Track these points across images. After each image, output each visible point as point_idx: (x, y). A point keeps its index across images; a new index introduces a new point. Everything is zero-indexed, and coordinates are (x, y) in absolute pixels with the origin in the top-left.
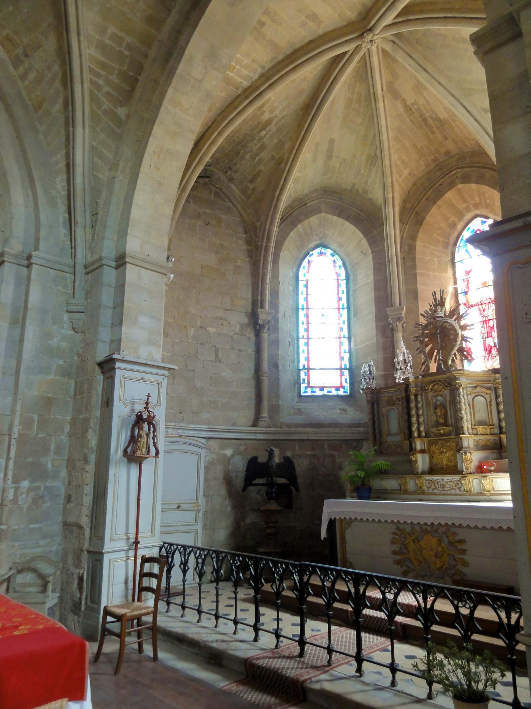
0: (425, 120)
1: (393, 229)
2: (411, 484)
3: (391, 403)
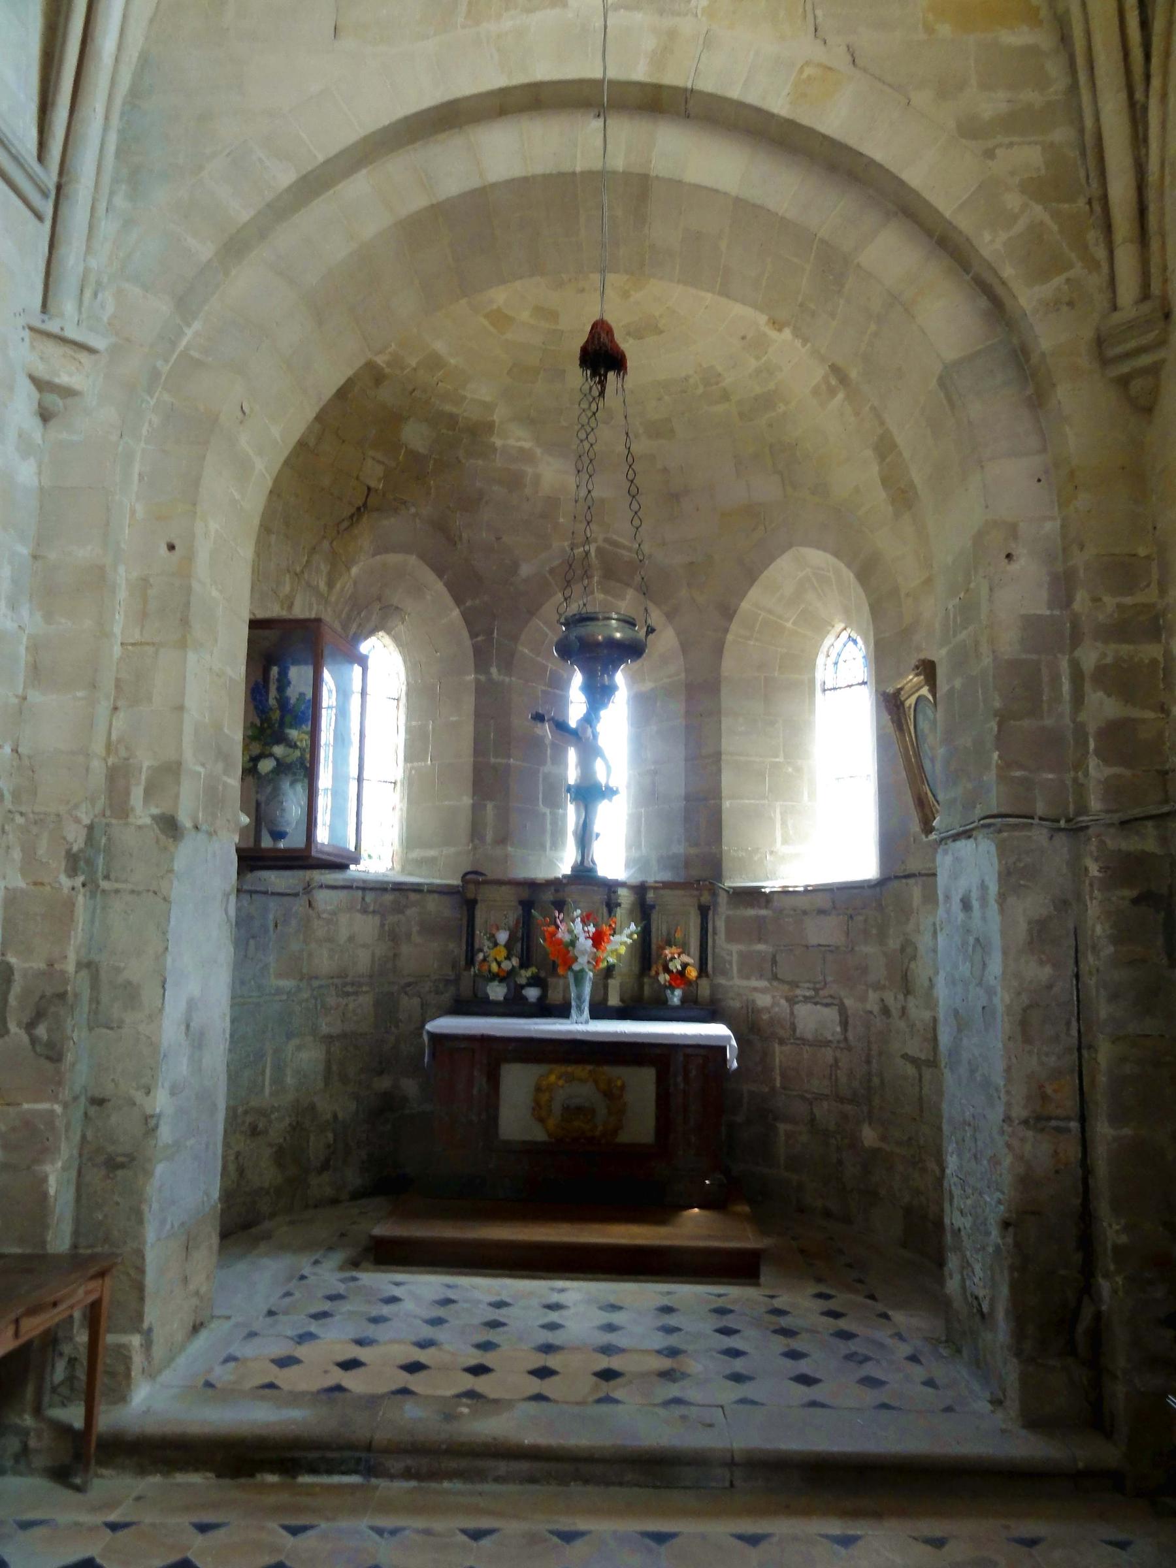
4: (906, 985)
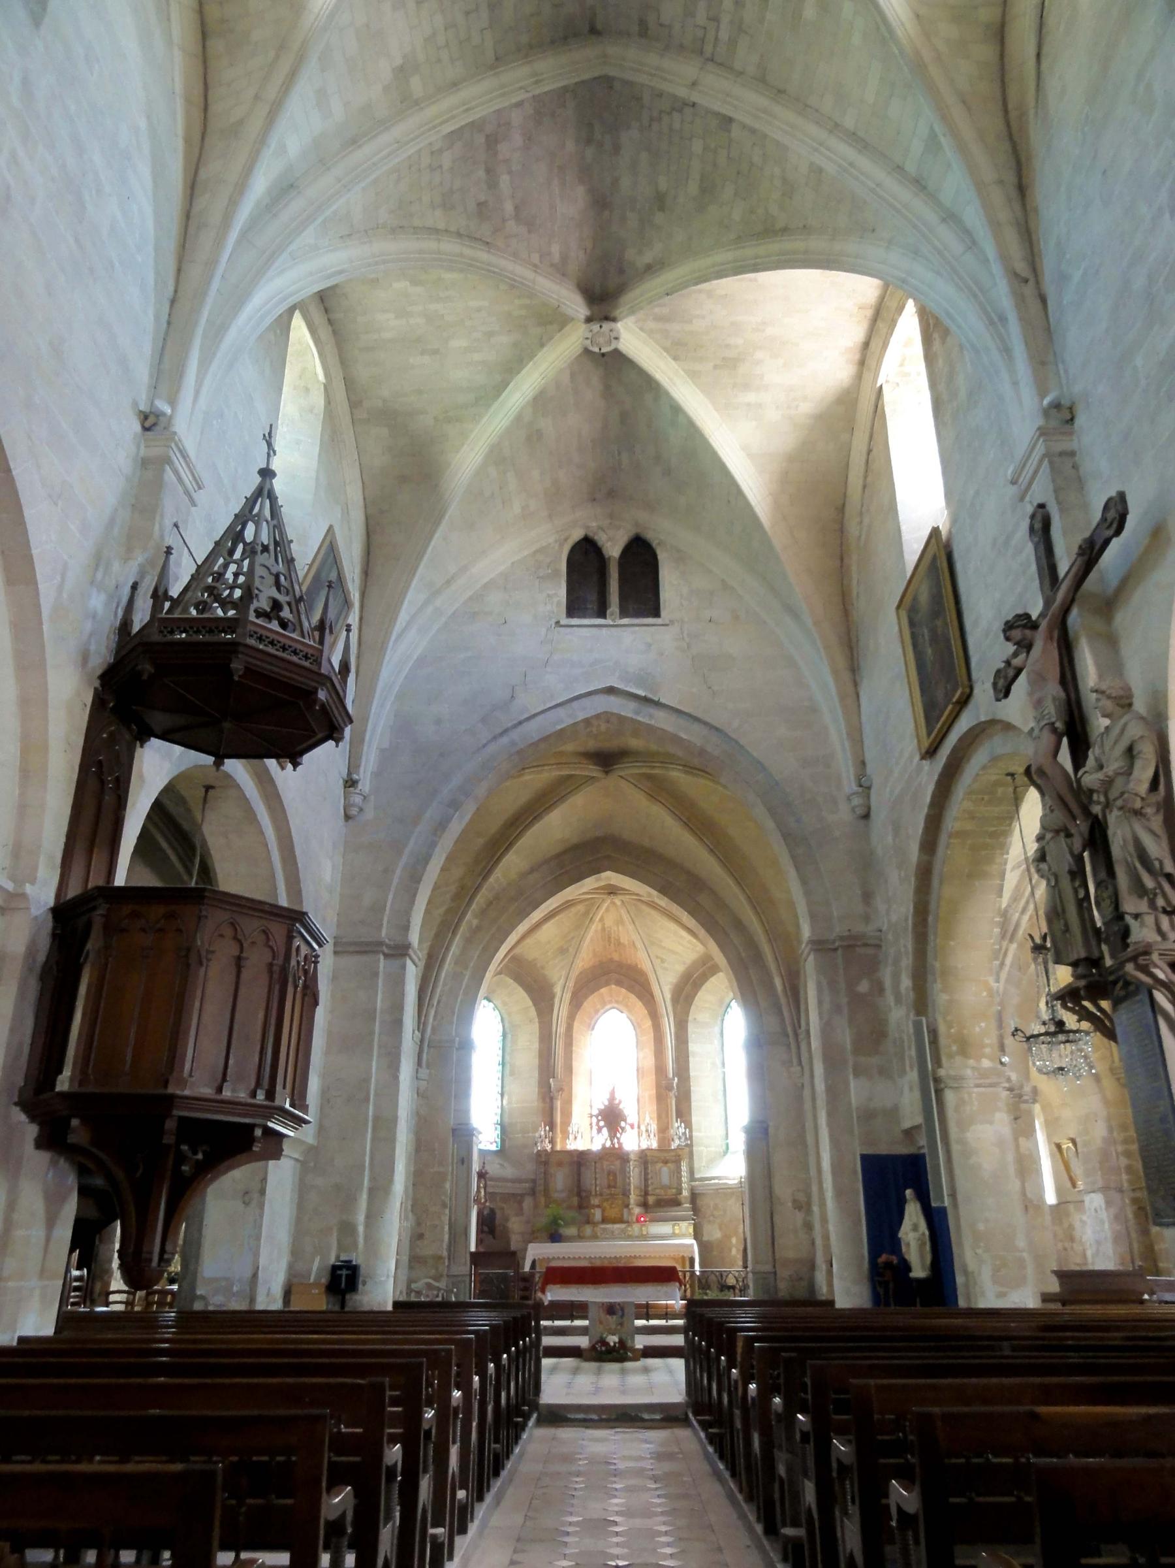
0: (610, 938)
1: (561, 1009)
2: (588, 1230)
3: (560, 1164)
4: (1072, 1239)
